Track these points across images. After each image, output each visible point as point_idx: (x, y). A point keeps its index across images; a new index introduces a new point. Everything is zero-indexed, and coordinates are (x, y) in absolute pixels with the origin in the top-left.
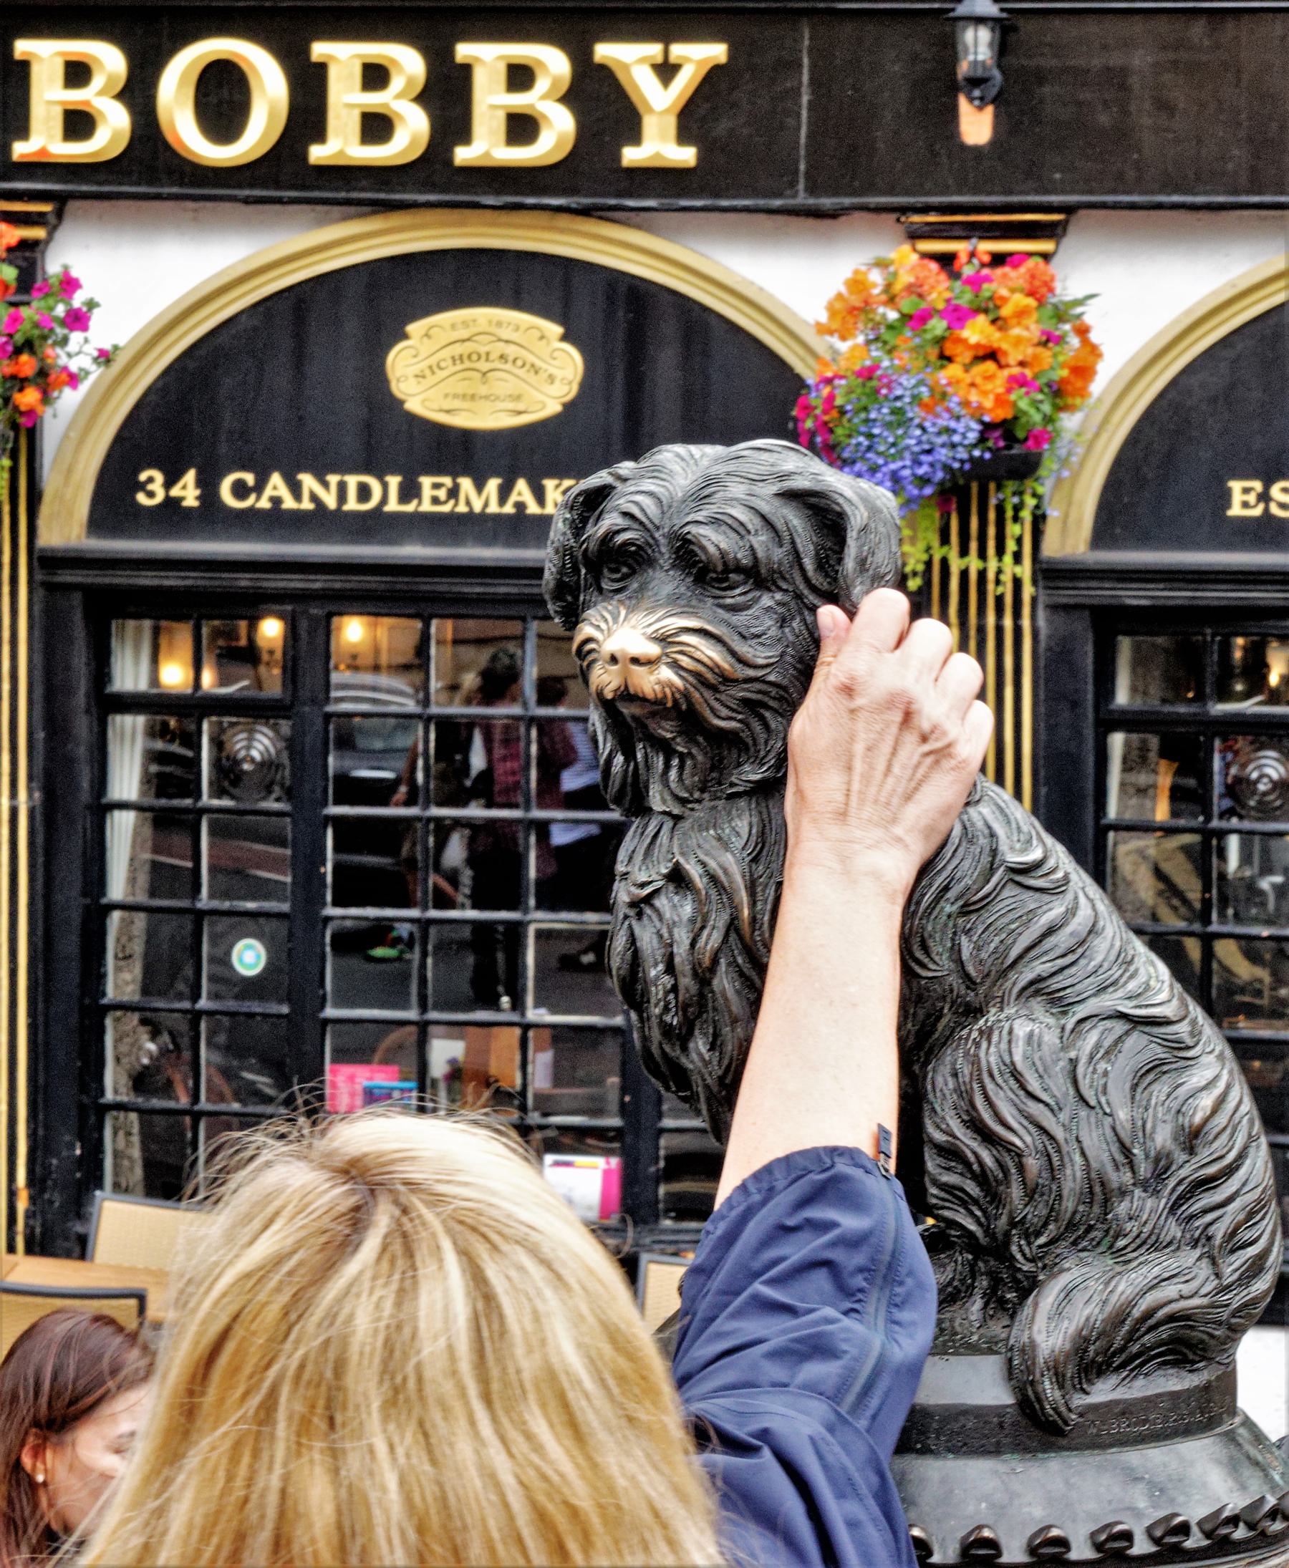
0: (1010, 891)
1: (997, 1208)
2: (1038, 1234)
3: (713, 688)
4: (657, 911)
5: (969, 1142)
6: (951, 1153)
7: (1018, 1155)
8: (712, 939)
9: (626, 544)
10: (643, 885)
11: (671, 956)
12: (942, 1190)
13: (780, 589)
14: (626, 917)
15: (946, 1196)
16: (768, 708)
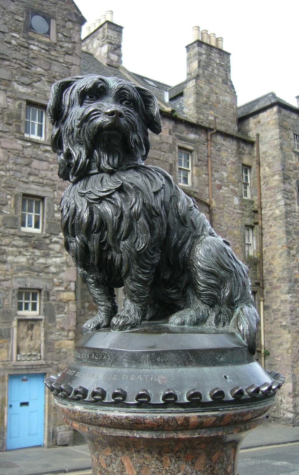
0: (194, 208)
1: (225, 290)
2: (236, 297)
3: (133, 131)
4: (114, 199)
5: (216, 269)
6: (210, 273)
7: (230, 272)
9: (102, 87)
10: (106, 192)
11: (122, 213)
13: (139, 113)
14: (89, 204)
15: (208, 287)
16: (138, 145)
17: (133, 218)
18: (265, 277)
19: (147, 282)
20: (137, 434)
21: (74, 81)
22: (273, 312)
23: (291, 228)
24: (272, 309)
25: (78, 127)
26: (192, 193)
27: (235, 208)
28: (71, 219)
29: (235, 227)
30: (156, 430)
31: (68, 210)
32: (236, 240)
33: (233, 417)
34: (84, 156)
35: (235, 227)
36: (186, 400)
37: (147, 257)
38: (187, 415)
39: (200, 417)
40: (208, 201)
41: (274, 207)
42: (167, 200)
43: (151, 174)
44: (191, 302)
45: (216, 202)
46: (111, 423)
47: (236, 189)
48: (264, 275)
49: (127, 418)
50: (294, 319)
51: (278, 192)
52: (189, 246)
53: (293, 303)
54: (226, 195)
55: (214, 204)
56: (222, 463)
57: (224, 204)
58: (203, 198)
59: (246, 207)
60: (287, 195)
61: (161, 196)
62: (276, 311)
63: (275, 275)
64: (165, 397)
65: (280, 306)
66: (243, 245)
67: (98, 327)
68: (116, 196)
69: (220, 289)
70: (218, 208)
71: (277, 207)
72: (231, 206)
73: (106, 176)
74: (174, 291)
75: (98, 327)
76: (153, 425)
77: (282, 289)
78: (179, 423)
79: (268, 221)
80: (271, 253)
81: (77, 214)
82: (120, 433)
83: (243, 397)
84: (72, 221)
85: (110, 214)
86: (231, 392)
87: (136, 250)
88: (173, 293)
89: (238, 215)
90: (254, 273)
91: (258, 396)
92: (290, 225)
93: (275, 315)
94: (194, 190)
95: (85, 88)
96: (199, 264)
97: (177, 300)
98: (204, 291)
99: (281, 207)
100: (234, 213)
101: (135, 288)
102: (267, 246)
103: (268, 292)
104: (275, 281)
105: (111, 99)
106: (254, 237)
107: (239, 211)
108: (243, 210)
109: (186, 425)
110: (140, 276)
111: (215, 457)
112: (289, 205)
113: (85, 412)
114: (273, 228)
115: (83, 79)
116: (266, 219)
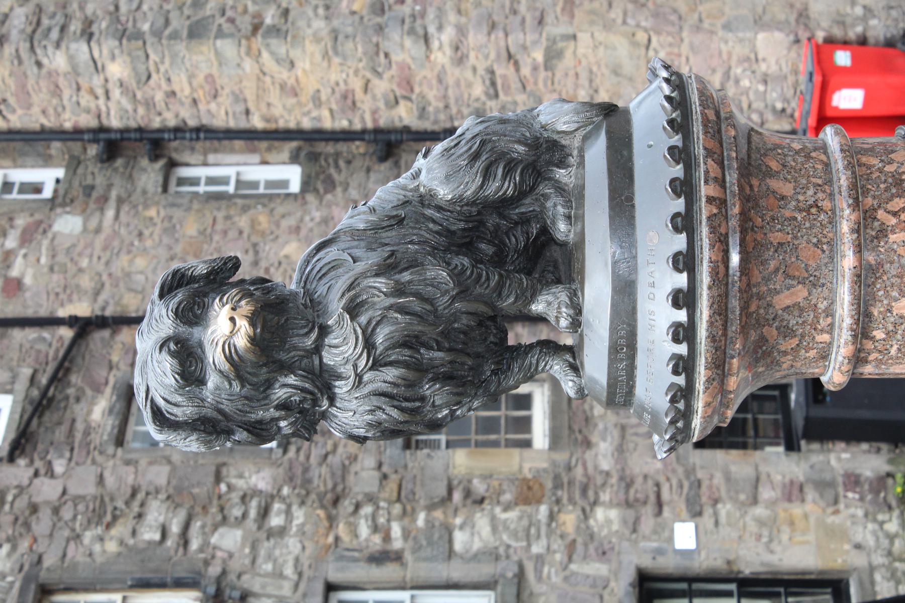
4: (369, 322)
5: (480, 165)
6: (487, 174)
7: (483, 143)
8: (381, 283)
11: (390, 307)
12: (505, 180)
15: (508, 179)
17: (399, 290)
18: (363, 119)
19: (501, 275)
20: (734, 275)
21: (152, 401)
22: (497, 96)
23: (177, 23)
24: (483, 98)
25: (243, 386)
26: (35, 393)
27: (98, 230)
28: (396, 403)
29: (170, 230)
30: (727, 245)
31: (380, 408)
32: (219, 226)
33: (709, 135)
34: (291, 380)
35: (170, 230)
36: (682, 200)
37: (463, 271)
38: (704, 200)
39: (706, 182)
40: (67, 333)
41: (97, 81)
42: (363, 244)
43: (318, 272)
44: (531, 209)
45: (70, 301)
46: (720, 315)
47: (21, 222)
48: (358, 126)
49: (710, 288)
50: (523, 21)
51: (39, 64)
52: (439, 212)
53: (463, 20)
54: (43, 260)
55: (82, 309)
56: (785, 156)
57: (81, 270)
58: (57, 350)
59: (92, 187)
60: (49, 29)
61: (358, 253)
62: (493, 84)
63: (357, 84)
64: (677, 230)
65: (474, 70)
66: (239, 201)
67: (576, 369)
68: (363, 319)
69: (513, 159)
70: (97, 293)
71: (97, 67)
72: (90, 245)
73: (329, 340)
74: (513, 239)
75: (576, 369)
76: (719, 249)
77: (409, 61)
78: (715, 211)
79: (149, 104)
80: (274, 96)
81: (390, 390)
82: (735, 303)
83: (679, 120)
84: (399, 401)
85: (393, 328)
86: (670, 138)
87: (453, 289)
88: (517, 240)
89: (123, 216)
90: (349, 162)
91: (678, 98)
92: (167, 22)
93: (507, 89)
94: (21, 385)
95: (178, 374)
96: (469, 193)
97: (528, 234)
98: (515, 184)
99: (96, 54)
100: (116, 233)
101: (511, 293)
102: (247, 112)
103: (422, 113)
104: (381, 86)
105: (196, 332)
106: (211, 158)
107: (110, 213)
108: (104, 199)
109: (720, 203)
110: (492, 284)
111: (774, 165)
112: (88, 23)
113: (706, 358)
114: (176, 87)
115: (152, 385)
116: (141, 111)
